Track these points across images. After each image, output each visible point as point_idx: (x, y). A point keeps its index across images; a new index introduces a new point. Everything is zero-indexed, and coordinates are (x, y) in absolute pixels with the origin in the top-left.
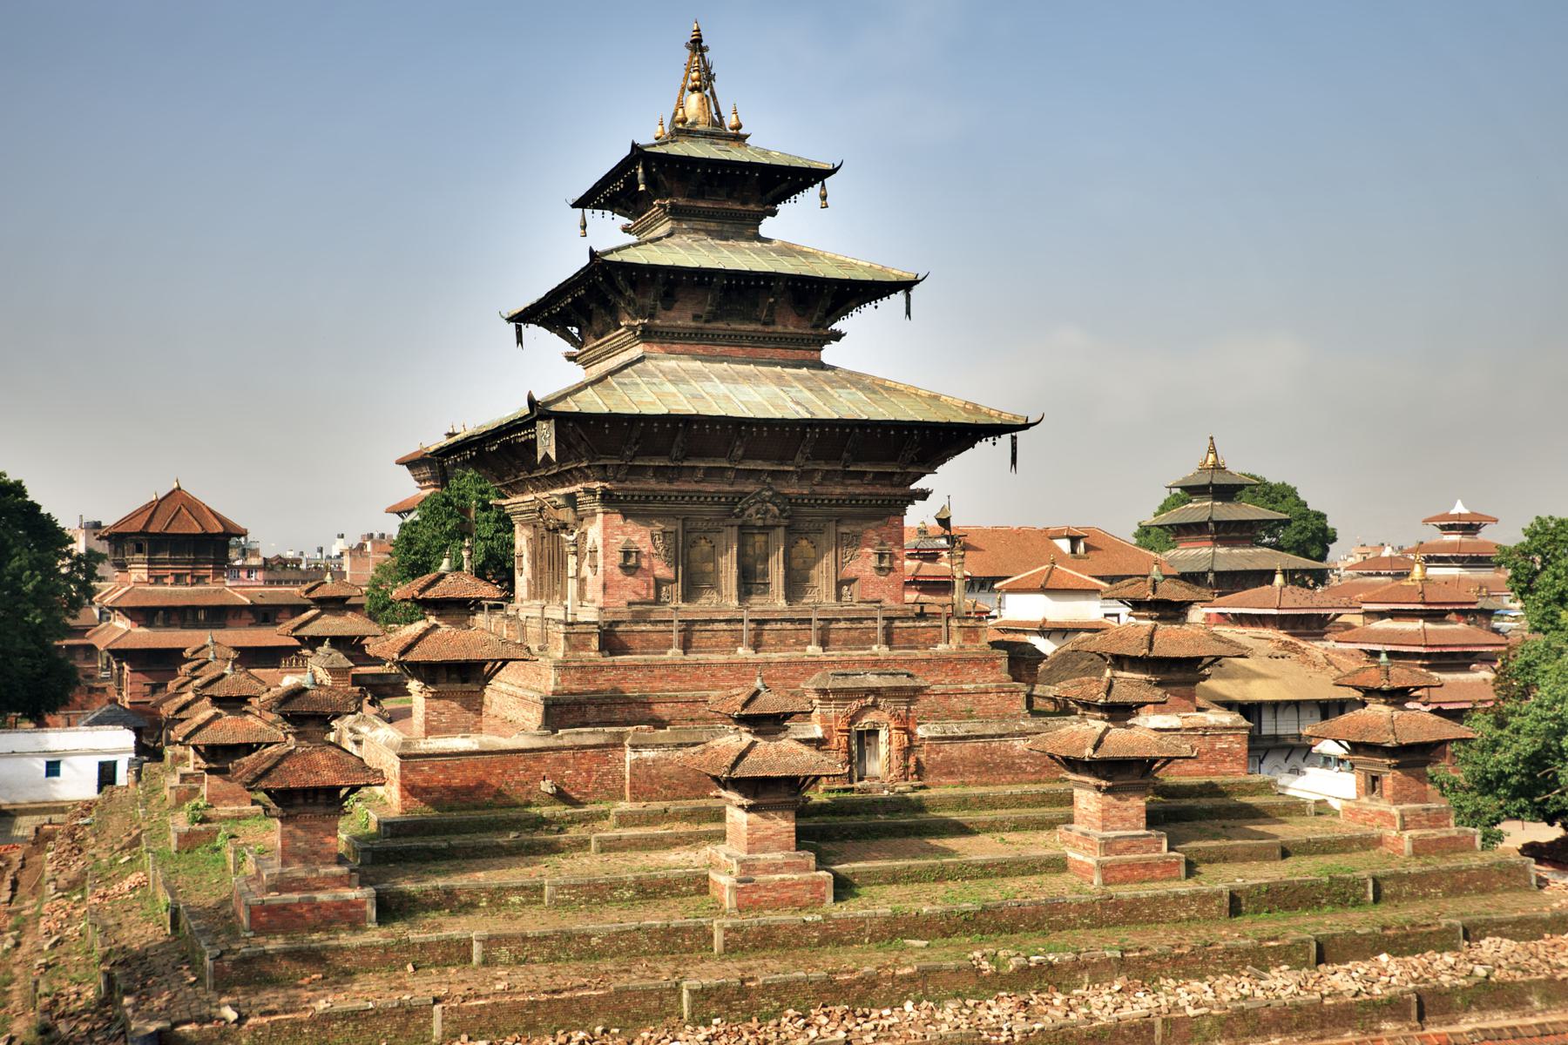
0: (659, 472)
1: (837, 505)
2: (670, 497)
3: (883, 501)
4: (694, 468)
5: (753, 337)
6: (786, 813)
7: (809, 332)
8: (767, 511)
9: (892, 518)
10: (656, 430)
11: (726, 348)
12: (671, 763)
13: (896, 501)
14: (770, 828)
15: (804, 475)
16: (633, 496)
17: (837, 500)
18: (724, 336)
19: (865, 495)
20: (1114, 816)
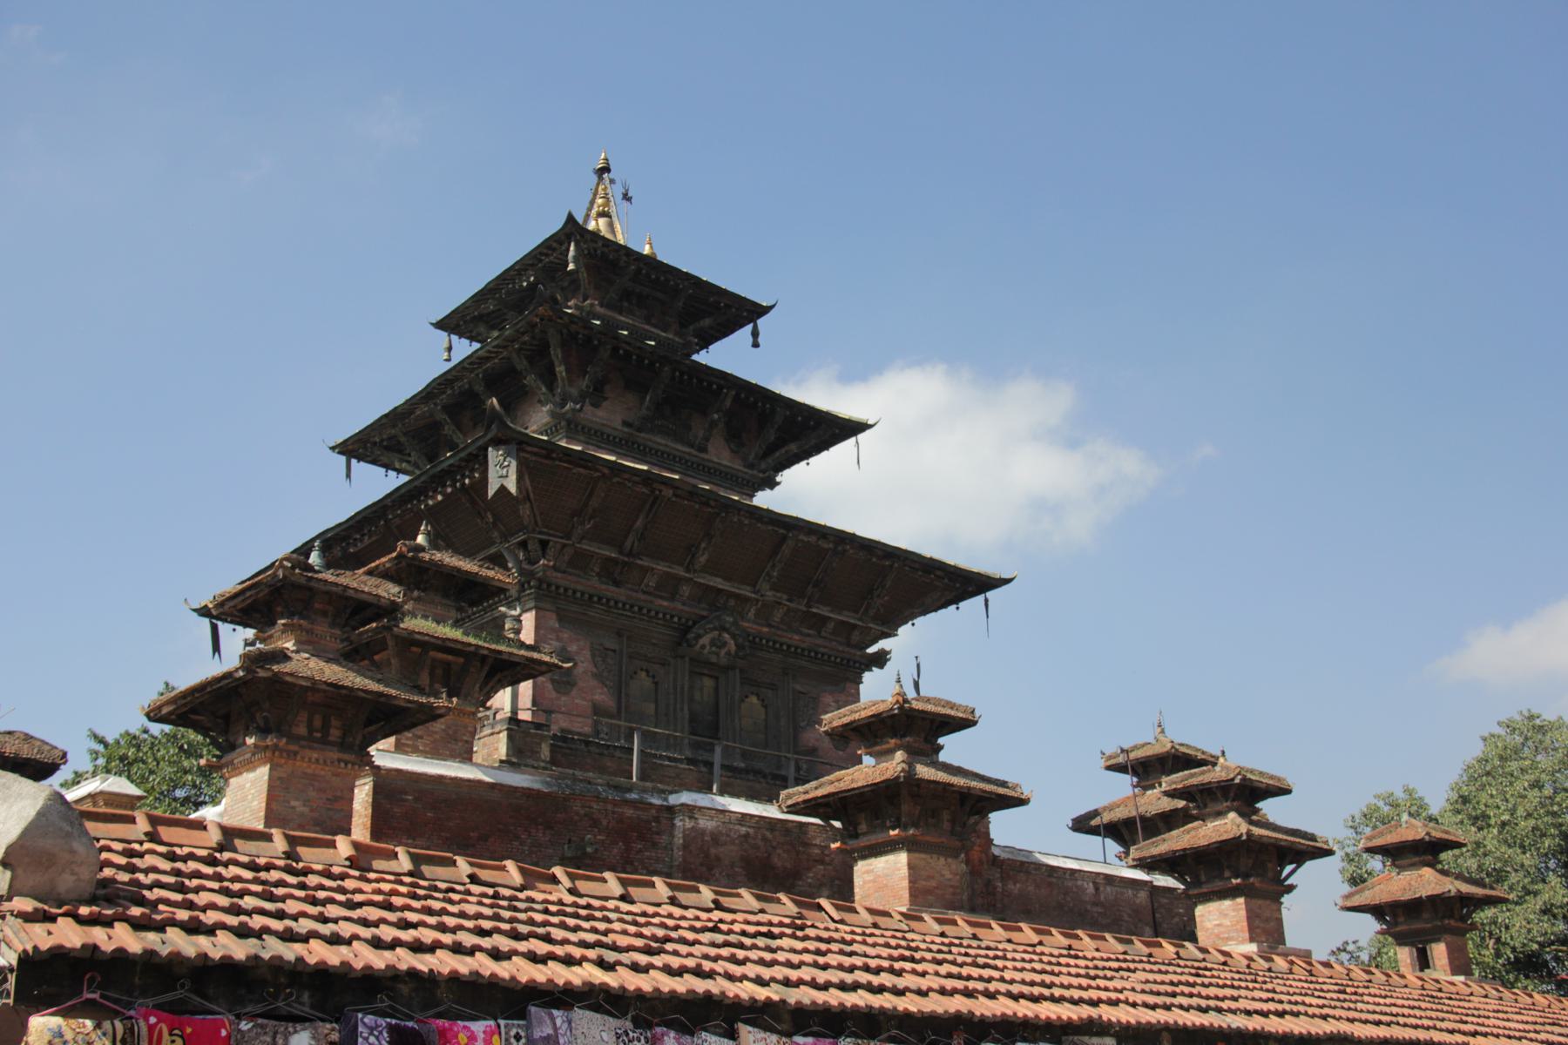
3: (842, 659)
5: (687, 461)
6: (950, 860)
7: (741, 468)
8: (725, 644)
9: (848, 685)
13: (855, 662)
18: (657, 451)
19: (825, 647)
20: (1258, 927)
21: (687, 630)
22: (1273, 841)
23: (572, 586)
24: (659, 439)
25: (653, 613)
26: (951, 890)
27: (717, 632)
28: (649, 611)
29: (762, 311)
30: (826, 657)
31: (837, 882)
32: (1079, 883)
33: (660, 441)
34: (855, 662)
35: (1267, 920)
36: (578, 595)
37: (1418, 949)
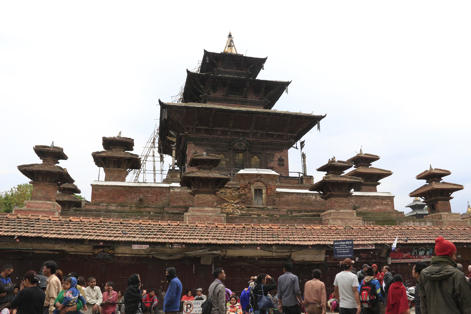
0: (206, 131)
1: (266, 145)
2: (210, 139)
3: (280, 144)
4: (217, 130)
5: (241, 101)
6: (211, 195)
7: (259, 100)
10: (200, 113)
11: (233, 104)
12: (185, 194)
13: (285, 144)
14: (205, 200)
15: (254, 135)
16: (197, 138)
17: (265, 143)
18: (232, 100)
19: (274, 141)
21: (232, 142)
22: (335, 181)
23: (196, 137)
24: (233, 98)
25: (220, 140)
26: (212, 202)
27: (239, 142)
28: (219, 140)
29: (264, 60)
30: (275, 144)
31: (219, 201)
32: (309, 196)
33: (233, 97)
34: (285, 144)
35: (341, 203)
36: (199, 139)
37: (432, 206)
